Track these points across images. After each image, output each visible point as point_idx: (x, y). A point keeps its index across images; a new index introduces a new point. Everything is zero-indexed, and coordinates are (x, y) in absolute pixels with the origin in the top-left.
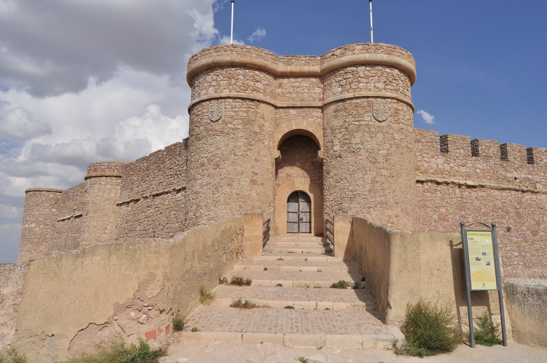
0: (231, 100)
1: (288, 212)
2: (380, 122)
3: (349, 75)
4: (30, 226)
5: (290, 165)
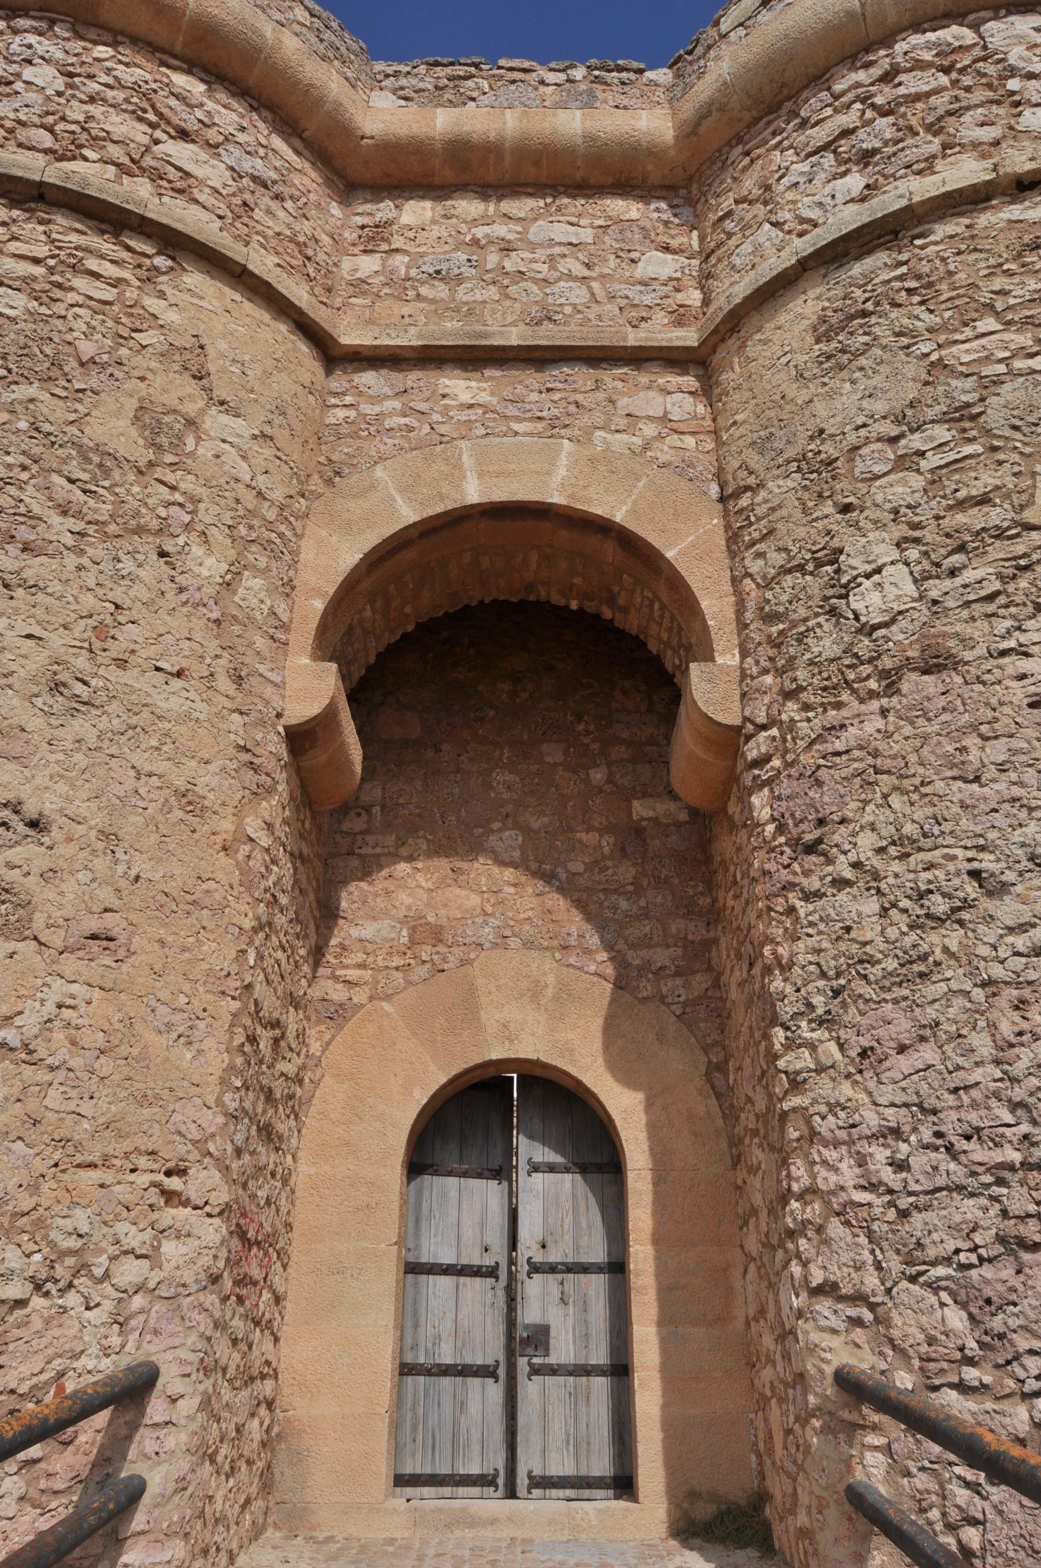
1: (414, 1269)
5: (440, 849)
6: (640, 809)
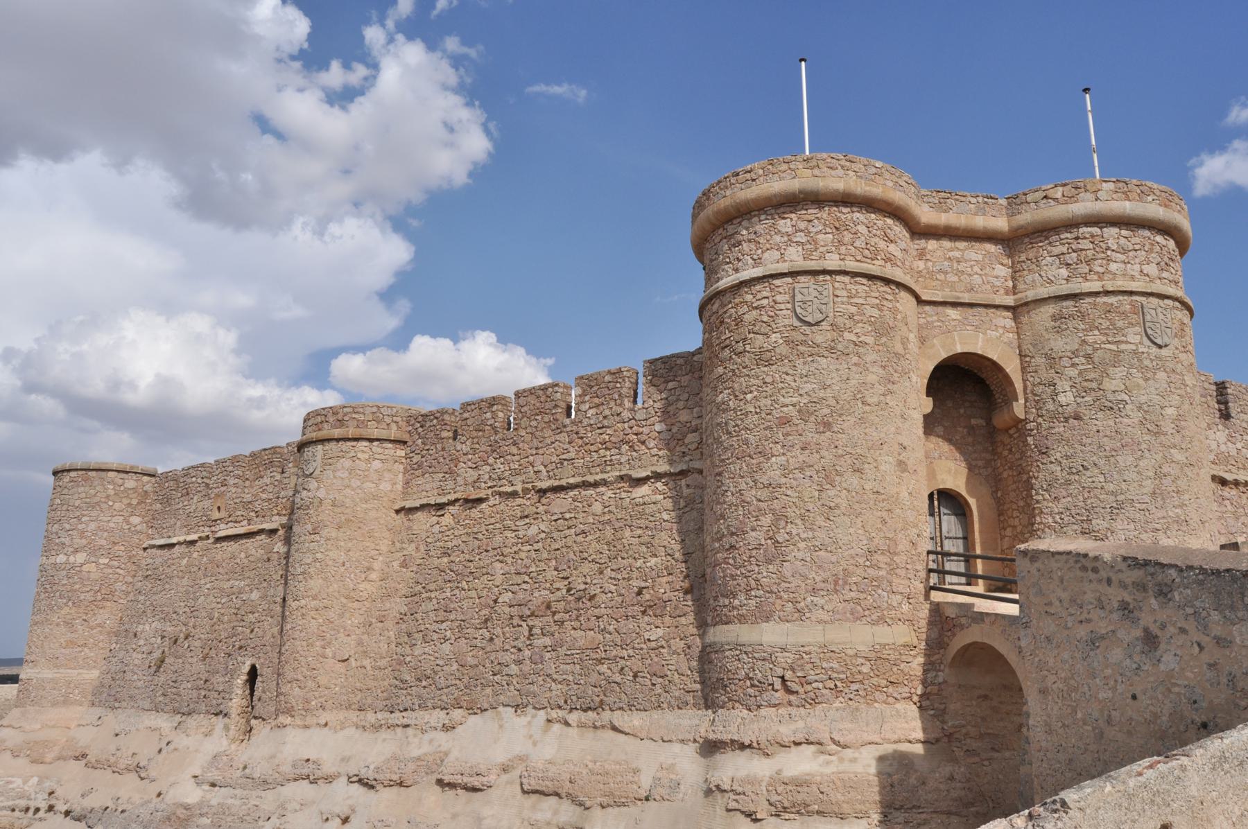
0: (847, 279)
2: (1160, 347)
3: (1085, 244)
4: (72, 559)
6: (973, 421)
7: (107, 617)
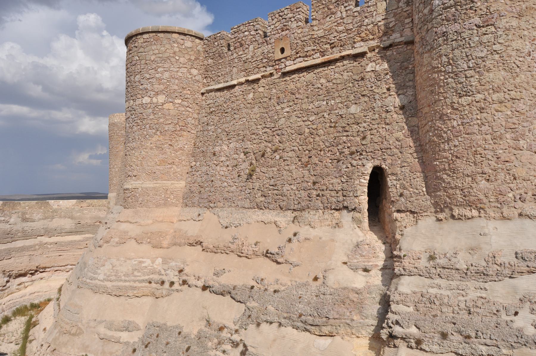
7: (185, 142)
